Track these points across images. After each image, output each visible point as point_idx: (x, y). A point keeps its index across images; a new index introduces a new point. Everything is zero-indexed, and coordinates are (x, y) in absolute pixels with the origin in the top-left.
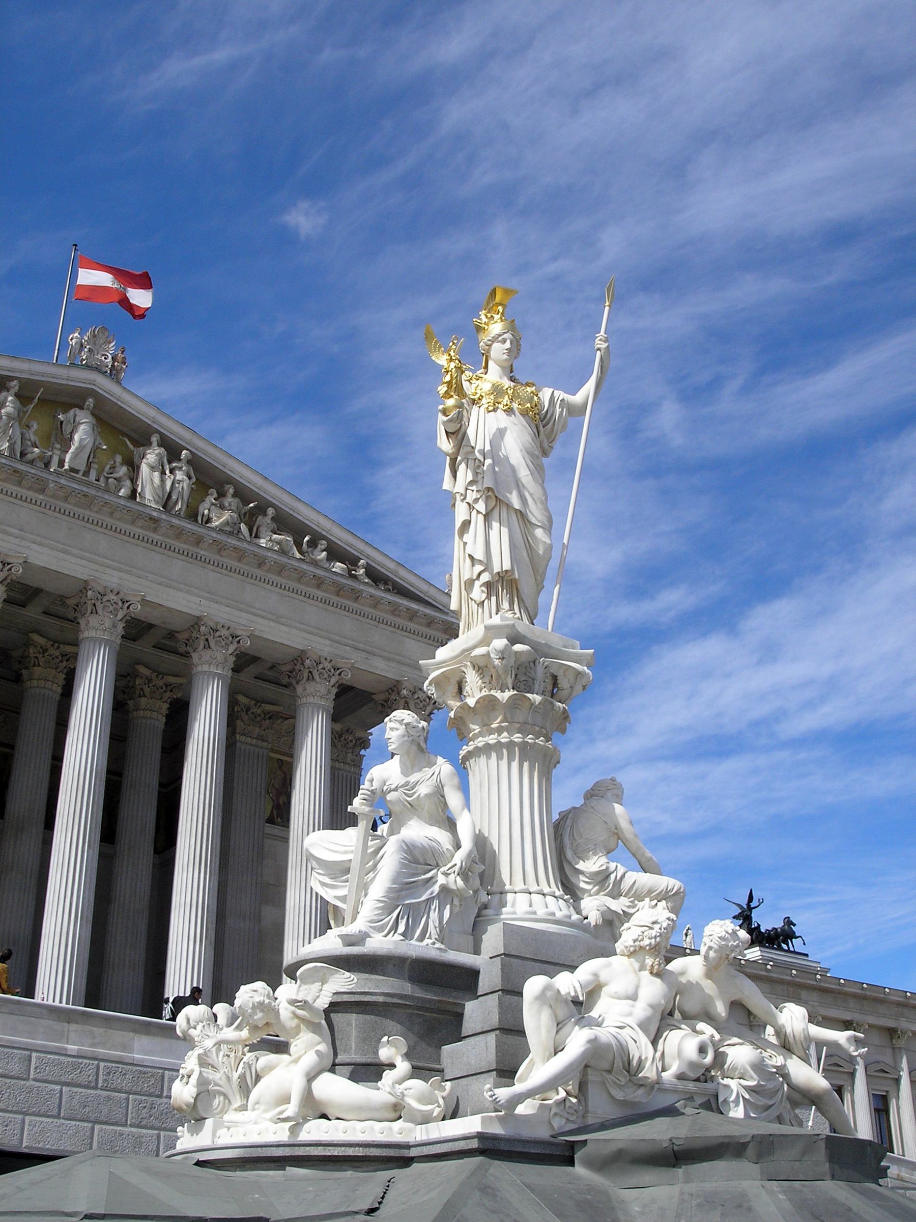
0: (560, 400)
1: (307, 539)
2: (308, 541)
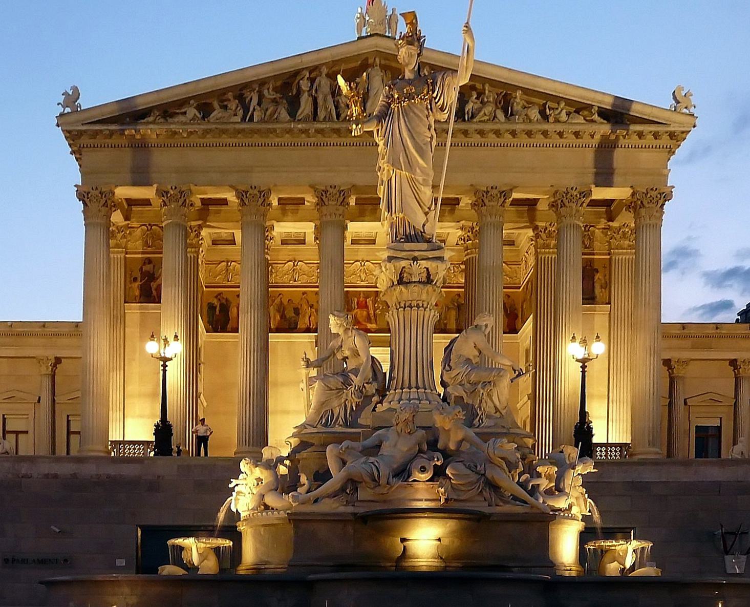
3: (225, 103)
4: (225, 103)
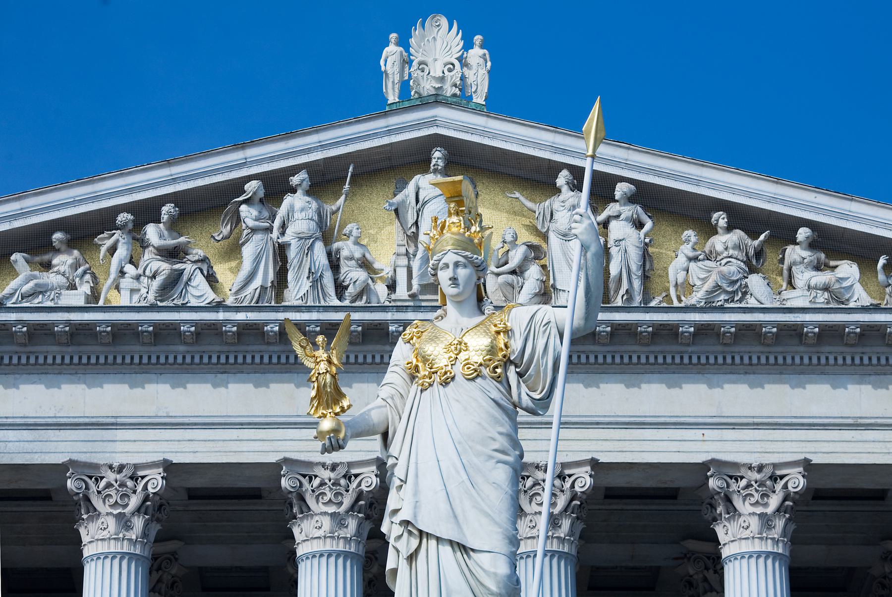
0: (543, 324)
1: (882, 261)
2: (885, 267)
4: (46, 257)
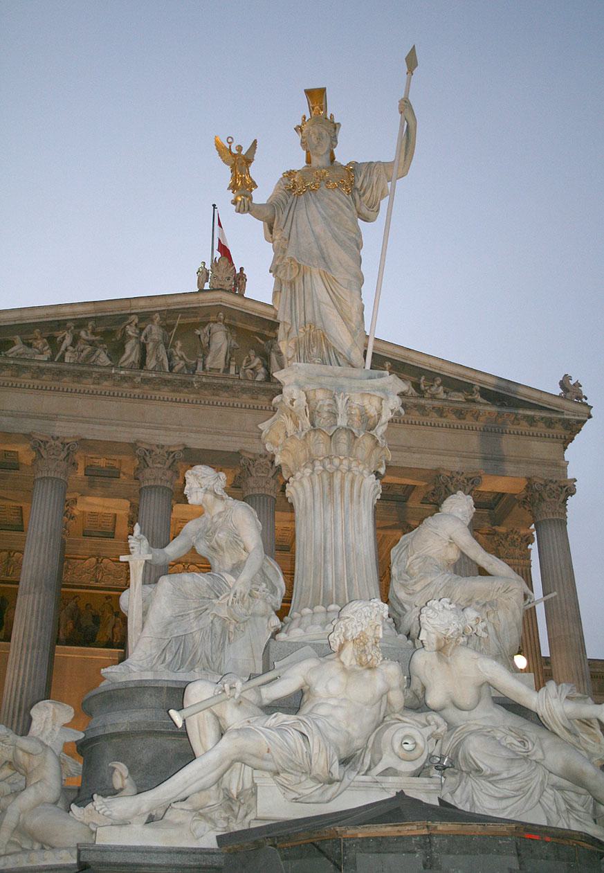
3: (30, 341)
